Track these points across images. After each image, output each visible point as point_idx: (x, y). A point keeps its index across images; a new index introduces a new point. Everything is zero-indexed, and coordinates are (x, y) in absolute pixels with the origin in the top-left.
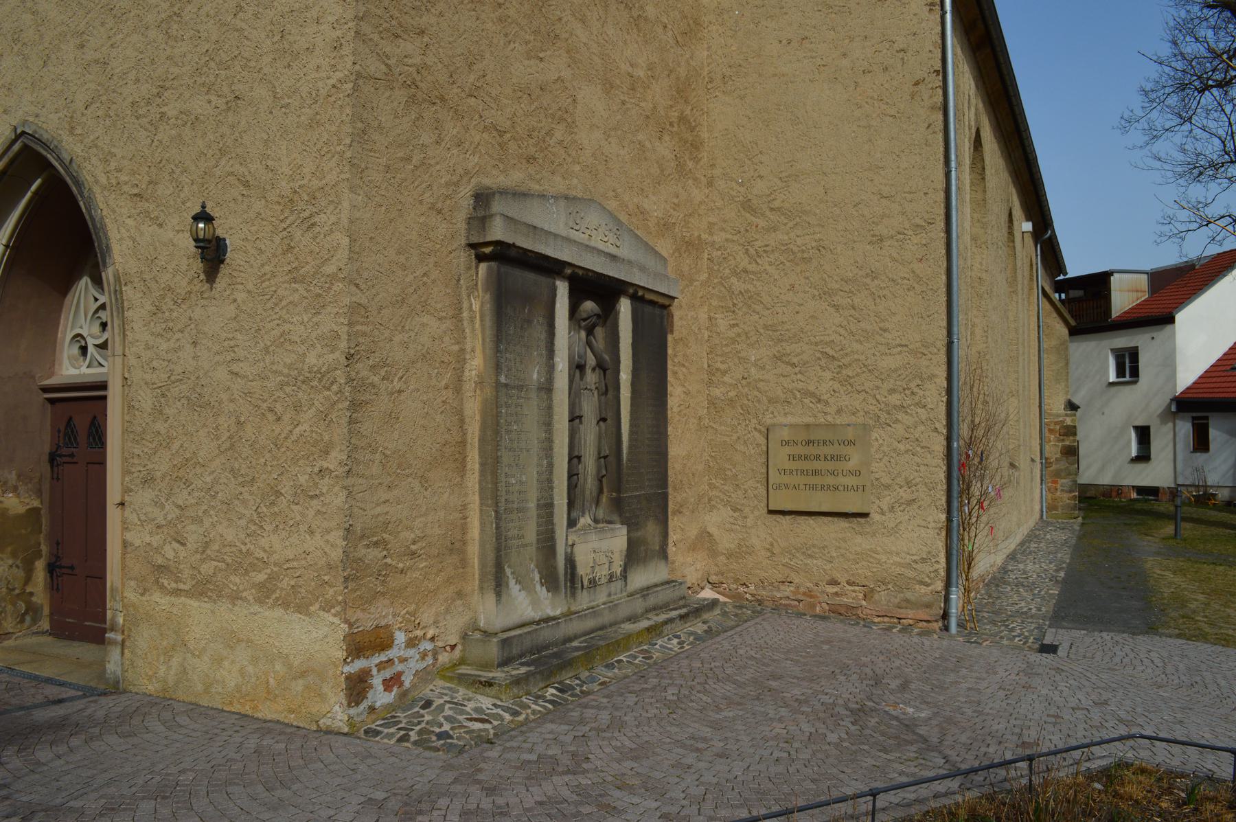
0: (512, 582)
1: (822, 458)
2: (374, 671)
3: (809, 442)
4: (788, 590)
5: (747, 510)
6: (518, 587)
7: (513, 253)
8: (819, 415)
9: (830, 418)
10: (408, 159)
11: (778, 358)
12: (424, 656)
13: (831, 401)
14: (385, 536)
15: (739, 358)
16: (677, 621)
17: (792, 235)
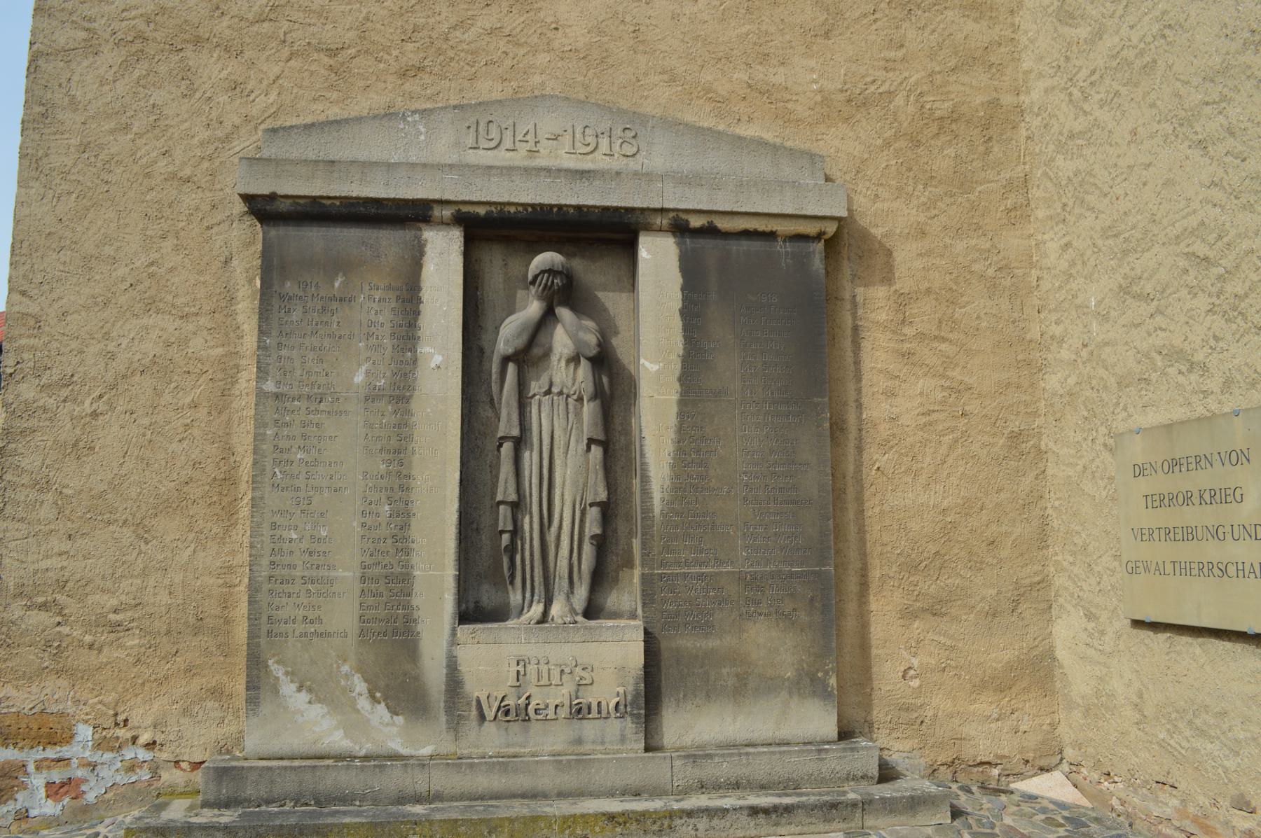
0: (287, 687)
1: (1196, 499)
2: (31, 768)
3: (1174, 464)
4: (1169, 804)
6: (304, 696)
7: (284, 206)
8: (1194, 399)
9: (1214, 407)
10: (127, 128)
11: (1125, 290)
12: (132, 767)
14: (58, 597)
15: (1078, 307)
16: (744, 818)
17: (1124, 31)
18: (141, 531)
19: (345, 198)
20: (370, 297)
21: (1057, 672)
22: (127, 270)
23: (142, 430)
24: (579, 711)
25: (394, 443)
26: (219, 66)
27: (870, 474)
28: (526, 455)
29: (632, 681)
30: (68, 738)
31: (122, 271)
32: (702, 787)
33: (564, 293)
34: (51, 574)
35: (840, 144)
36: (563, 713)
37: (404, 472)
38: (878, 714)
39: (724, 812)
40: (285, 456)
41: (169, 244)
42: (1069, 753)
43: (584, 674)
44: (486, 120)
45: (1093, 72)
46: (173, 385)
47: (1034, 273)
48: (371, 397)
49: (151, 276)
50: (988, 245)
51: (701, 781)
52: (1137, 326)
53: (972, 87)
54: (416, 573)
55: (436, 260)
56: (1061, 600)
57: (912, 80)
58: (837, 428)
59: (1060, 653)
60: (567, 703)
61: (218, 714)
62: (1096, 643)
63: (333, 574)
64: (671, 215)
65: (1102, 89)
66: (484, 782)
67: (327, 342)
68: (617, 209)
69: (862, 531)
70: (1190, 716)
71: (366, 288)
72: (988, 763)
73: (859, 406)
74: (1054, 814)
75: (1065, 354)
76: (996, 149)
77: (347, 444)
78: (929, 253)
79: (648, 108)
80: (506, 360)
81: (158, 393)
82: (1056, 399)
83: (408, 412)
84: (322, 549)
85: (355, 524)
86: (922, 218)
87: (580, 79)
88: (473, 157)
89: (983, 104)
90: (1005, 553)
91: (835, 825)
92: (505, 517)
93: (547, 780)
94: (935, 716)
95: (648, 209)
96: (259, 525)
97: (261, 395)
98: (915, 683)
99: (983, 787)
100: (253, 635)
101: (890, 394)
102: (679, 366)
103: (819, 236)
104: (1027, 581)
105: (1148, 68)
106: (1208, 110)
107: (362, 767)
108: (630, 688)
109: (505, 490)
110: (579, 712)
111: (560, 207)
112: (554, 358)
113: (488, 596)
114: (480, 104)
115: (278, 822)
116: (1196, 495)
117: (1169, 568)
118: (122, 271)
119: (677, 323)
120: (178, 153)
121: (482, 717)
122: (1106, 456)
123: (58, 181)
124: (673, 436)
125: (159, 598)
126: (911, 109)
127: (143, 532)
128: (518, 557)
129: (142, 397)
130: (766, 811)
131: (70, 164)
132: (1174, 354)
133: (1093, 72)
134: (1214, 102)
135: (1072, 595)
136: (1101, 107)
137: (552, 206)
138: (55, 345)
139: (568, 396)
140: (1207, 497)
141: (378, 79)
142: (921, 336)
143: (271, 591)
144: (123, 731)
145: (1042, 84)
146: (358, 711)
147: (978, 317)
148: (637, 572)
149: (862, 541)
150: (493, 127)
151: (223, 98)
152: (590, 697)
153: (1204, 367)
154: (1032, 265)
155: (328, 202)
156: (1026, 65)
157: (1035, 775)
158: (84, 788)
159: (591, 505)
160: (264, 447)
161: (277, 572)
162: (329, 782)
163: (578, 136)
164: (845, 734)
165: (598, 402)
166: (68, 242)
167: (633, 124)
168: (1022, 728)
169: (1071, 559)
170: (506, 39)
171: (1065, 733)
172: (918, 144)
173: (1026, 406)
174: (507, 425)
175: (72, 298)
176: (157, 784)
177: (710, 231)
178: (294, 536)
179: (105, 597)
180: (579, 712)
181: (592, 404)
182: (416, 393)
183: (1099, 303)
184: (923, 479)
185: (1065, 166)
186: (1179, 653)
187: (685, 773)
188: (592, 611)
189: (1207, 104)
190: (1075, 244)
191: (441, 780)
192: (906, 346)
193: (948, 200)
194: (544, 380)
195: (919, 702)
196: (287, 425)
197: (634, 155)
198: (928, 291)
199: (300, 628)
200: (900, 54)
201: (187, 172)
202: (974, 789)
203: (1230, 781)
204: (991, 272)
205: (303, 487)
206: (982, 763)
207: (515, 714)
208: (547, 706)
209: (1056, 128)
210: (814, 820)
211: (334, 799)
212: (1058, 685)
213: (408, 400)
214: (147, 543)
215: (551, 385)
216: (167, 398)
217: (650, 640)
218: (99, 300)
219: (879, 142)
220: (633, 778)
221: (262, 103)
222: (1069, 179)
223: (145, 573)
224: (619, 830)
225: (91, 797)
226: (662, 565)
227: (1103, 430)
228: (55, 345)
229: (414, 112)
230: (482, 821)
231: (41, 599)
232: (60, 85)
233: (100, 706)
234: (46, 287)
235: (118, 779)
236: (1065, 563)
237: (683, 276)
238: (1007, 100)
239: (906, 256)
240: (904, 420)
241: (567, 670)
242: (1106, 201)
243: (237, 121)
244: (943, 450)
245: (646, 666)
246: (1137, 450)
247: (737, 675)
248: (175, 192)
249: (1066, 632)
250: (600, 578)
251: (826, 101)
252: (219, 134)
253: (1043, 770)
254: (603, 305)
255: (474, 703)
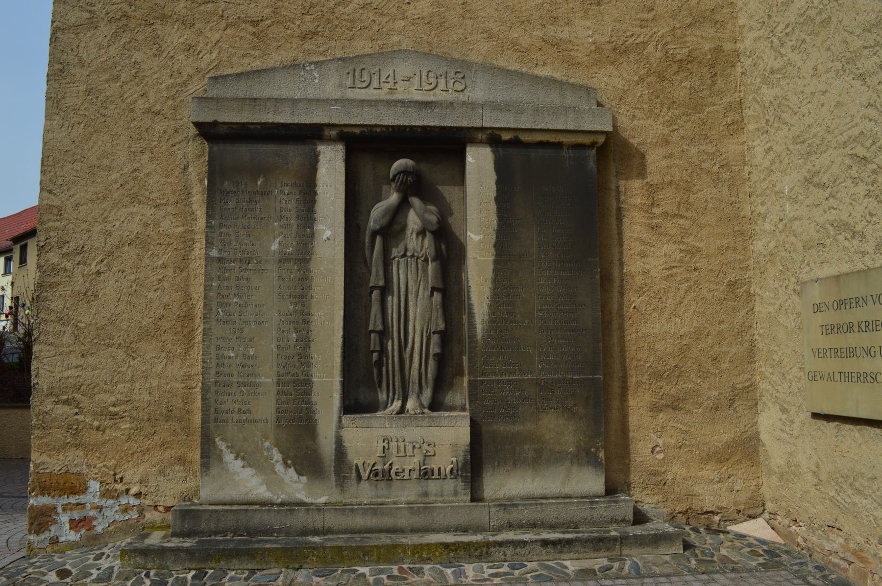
0: (229, 457)
1: (856, 329)
2: (60, 510)
3: (841, 304)
4: (836, 542)
5: (793, 410)
6: (239, 463)
7: (223, 130)
9: (869, 263)
10: (117, 78)
12: (126, 509)
13: (869, 231)
14: (76, 395)
15: (776, 193)
16: (538, 548)
18: (130, 352)
19: (264, 123)
20: (281, 191)
21: (761, 449)
22: (118, 175)
23: (130, 284)
24: (426, 474)
25: (298, 291)
26: (179, 34)
27: (629, 311)
28: (390, 298)
29: (462, 454)
30: (84, 490)
31: (115, 176)
32: (511, 526)
33: (415, 187)
34: (70, 380)
35: (607, 80)
36: (415, 475)
37: (306, 311)
38: (635, 477)
39: (523, 543)
40: (226, 300)
41: (146, 157)
42: (769, 506)
43: (428, 448)
44: (360, 68)
45: (787, 26)
46: (150, 253)
47: (747, 169)
48: (283, 260)
49: (135, 179)
50: (713, 150)
51: (509, 522)
52: (816, 206)
53: (702, 38)
54: (314, 379)
55: (326, 165)
56: (764, 399)
57: (660, 34)
58: (606, 280)
59: (764, 437)
60: (417, 468)
61: (183, 474)
62: (787, 429)
63: (258, 380)
64: (488, 132)
65: (793, 38)
66: (360, 521)
67: (253, 223)
68: (451, 128)
69: (623, 350)
70: (851, 480)
71: (279, 185)
72: (712, 512)
73: (621, 264)
74: (755, 547)
75: (768, 226)
76: (719, 82)
77: (266, 291)
78: (671, 156)
79: (473, 57)
80: (374, 234)
81: (140, 258)
82: (761, 258)
83: (308, 270)
84: (251, 363)
85: (273, 346)
86: (666, 131)
87: (426, 37)
88: (351, 94)
89: (710, 50)
90: (724, 366)
91: (601, 553)
92: (375, 341)
93: (403, 521)
94: (674, 479)
95: (472, 128)
96: (208, 347)
97: (208, 259)
98: (660, 456)
99: (708, 529)
100: (205, 421)
101: (643, 255)
102: (494, 237)
103: (593, 145)
104: (740, 386)
105: (825, 23)
106: (866, 52)
107: (278, 510)
108: (461, 458)
109: (375, 322)
110: (426, 474)
111: (411, 127)
112: (408, 232)
113: (363, 396)
114: (356, 57)
115: (221, 547)
116: (856, 325)
117: (837, 376)
118: (115, 176)
119: (493, 207)
120: (151, 94)
121: (359, 478)
122: (795, 297)
123: (72, 115)
124: (490, 285)
125: (142, 396)
126: (658, 54)
127: (131, 352)
128: (384, 369)
129: (129, 261)
130: (554, 543)
131: (79, 103)
132: (843, 226)
133: (787, 26)
134: (871, 47)
135: (771, 395)
136: (793, 51)
137: (405, 127)
138: (71, 226)
139: (418, 258)
140: (863, 326)
141: (286, 41)
142: (665, 215)
143: (216, 392)
144: (120, 485)
145: (753, 35)
146: (275, 473)
147: (706, 201)
148: (466, 379)
149: (623, 358)
150: (365, 73)
151: (181, 56)
152: (433, 464)
153: (863, 235)
154: (745, 164)
155: (253, 127)
156: (741, 22)
157: (745, 521)
158: (94, 523)
159: (434, 333)
160: (211, 294)
161: (221, 379)
162: (256, 521)
163: (424, 78)
164: (611, 490)
165: (438, 262)
166: (79, 157)
167: (462, 68)
168: (736, 488)
169: (771, 370)
170: (374, 11)
171: (766, 492)
172: (664, 79)
173: (740, 263)
174: (376, 278)
175: (82, 194)
176: (142, 521)
177: (516, 143)
178: (232, 355)
179: (107, 396)
180: (426, 474)
181: (434, 264)
182: (314, 257)
183: (791, 190)
184: (666, 314)
185: (768, 93)
186: (844, 436)
187: (499, 517)
188: (436, 405)
189: (866, 48)
190: (775, 148)
191: (332, 520)
192: (655, 221)
193: (685, 118)
194: (401, 246)
195: (663, 469)
196: (226, 279)
197: (462, 91)
198: (671, 183)
199: (236, 417)
200: (651, 15)
201: (158, 107)
202: (702, 530)
203: (878, 525)
204: (715, 169)
205: (238, 321)
206: (707, 512)
207: (383, 476)
208: (404, 470)
209: (761, 67)
210: (586, 550)
211: (260, 532)
212: (762, 458)
213: (308, 261)
214: (134, 360)
215: (406, 250)
216: (146, 261)
217: (475, 427)
218: (100, 195)
219: (636, 78)
220: (462, 519)
221: (208, 59)
222: (771, 102)
223: (133, 380)
224: (452, 554)
225: (99, 529)
226: (483, 374)
227: (793, 280)
228: (71, 226)
229: (311, 64)
230: (358, 547)
231: (64, 397)
232: (72, 50)
233: (104, 469)
234: (65, 187)
235: (117, 517)
236: (767, 373)
237: (497, 174)
238: (728, 46)
239: (654, 158)
240: (653, 273)
241: (417, 446)
242: (796, 117)
243: (191, 72)
244: (681, 294)
245: (472, 443)
246: (816, 294)
247: (535, 450)
248: (150, 121)
249: (768, 421)
250: (442, 384)
251: (598, 49)
252: (179, 81)
253: (751, 517)
254: (442, 195)
255: (354, 468)
